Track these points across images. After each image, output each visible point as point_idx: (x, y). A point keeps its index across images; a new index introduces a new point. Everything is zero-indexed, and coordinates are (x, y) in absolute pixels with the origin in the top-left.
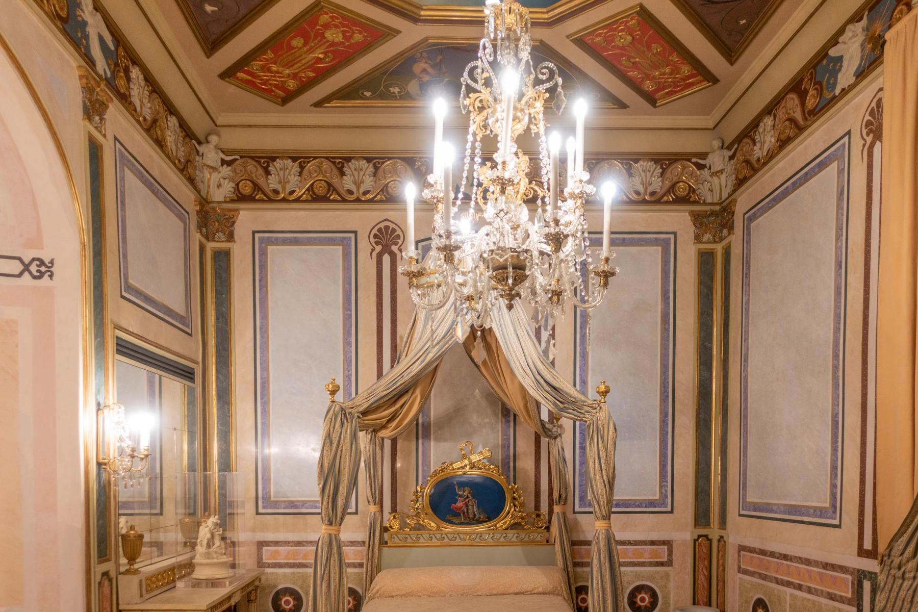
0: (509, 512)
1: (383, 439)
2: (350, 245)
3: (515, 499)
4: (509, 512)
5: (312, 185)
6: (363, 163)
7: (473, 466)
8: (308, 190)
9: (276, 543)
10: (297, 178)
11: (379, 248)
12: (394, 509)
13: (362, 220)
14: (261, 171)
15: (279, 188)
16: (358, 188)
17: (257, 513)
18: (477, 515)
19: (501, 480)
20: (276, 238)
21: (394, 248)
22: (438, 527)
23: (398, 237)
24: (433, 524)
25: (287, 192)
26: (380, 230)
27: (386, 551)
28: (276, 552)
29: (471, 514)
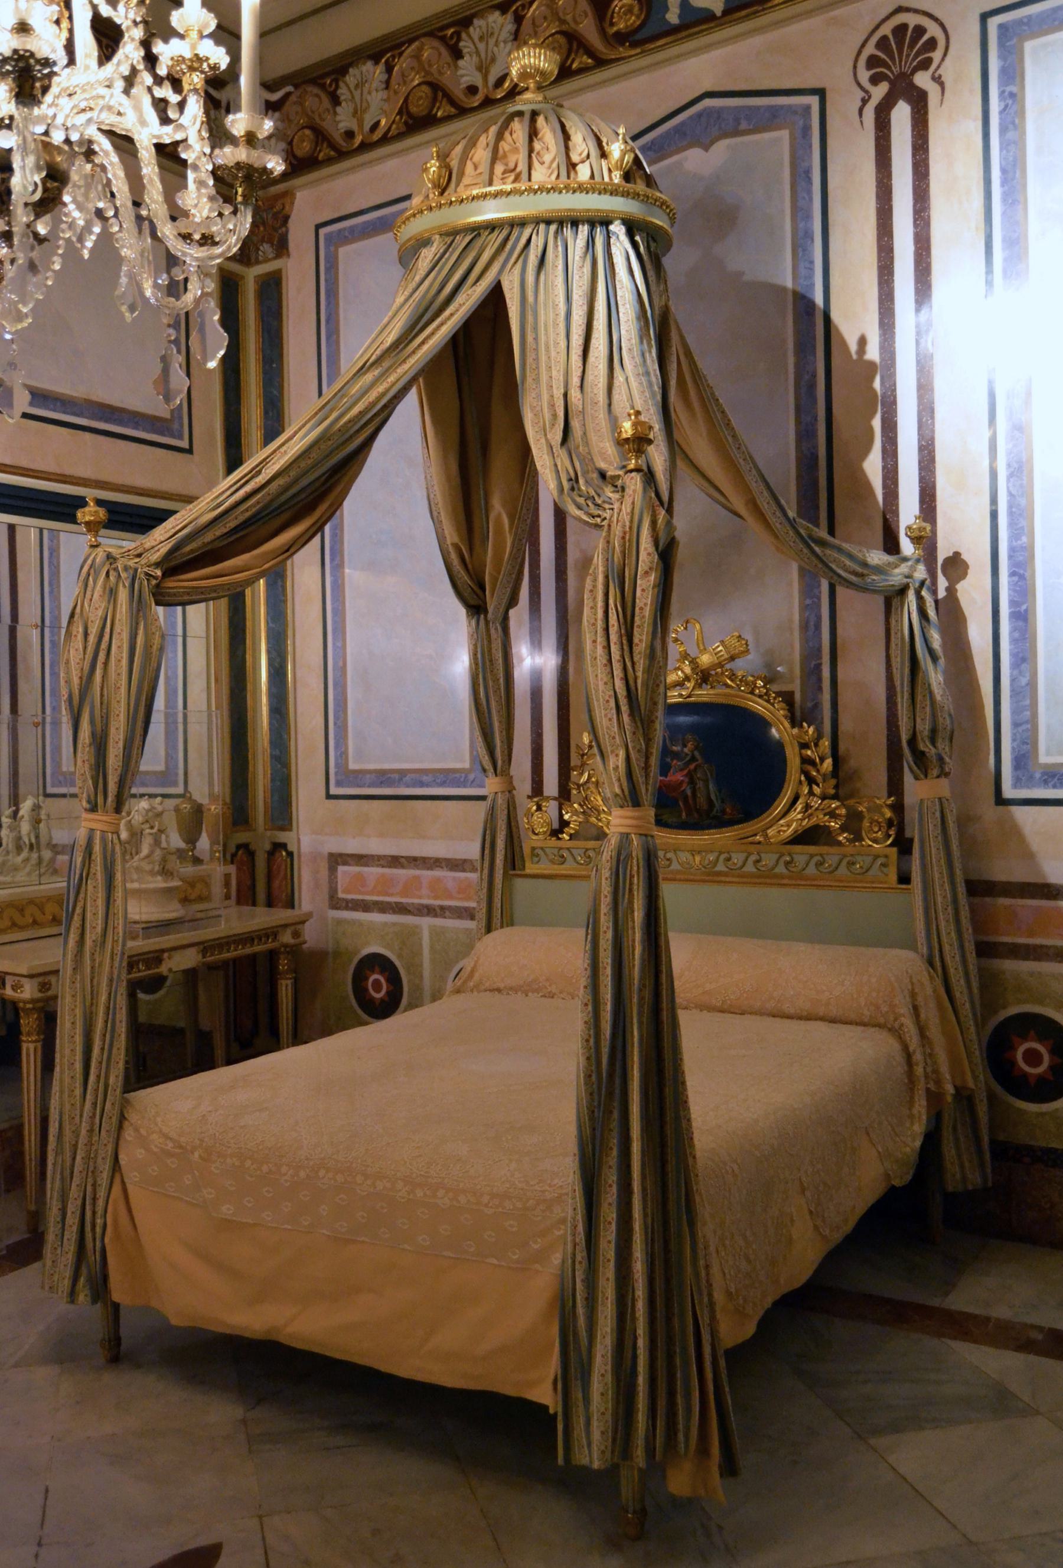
3: (806, 761)
9: (361, 859)
14: (326, 103)
15: (355, 127)
17: (329, 796)
18: (717, 804)
20: (352, 229)
27: (519, 884)
28: (360, 878)
29: (702, 800)
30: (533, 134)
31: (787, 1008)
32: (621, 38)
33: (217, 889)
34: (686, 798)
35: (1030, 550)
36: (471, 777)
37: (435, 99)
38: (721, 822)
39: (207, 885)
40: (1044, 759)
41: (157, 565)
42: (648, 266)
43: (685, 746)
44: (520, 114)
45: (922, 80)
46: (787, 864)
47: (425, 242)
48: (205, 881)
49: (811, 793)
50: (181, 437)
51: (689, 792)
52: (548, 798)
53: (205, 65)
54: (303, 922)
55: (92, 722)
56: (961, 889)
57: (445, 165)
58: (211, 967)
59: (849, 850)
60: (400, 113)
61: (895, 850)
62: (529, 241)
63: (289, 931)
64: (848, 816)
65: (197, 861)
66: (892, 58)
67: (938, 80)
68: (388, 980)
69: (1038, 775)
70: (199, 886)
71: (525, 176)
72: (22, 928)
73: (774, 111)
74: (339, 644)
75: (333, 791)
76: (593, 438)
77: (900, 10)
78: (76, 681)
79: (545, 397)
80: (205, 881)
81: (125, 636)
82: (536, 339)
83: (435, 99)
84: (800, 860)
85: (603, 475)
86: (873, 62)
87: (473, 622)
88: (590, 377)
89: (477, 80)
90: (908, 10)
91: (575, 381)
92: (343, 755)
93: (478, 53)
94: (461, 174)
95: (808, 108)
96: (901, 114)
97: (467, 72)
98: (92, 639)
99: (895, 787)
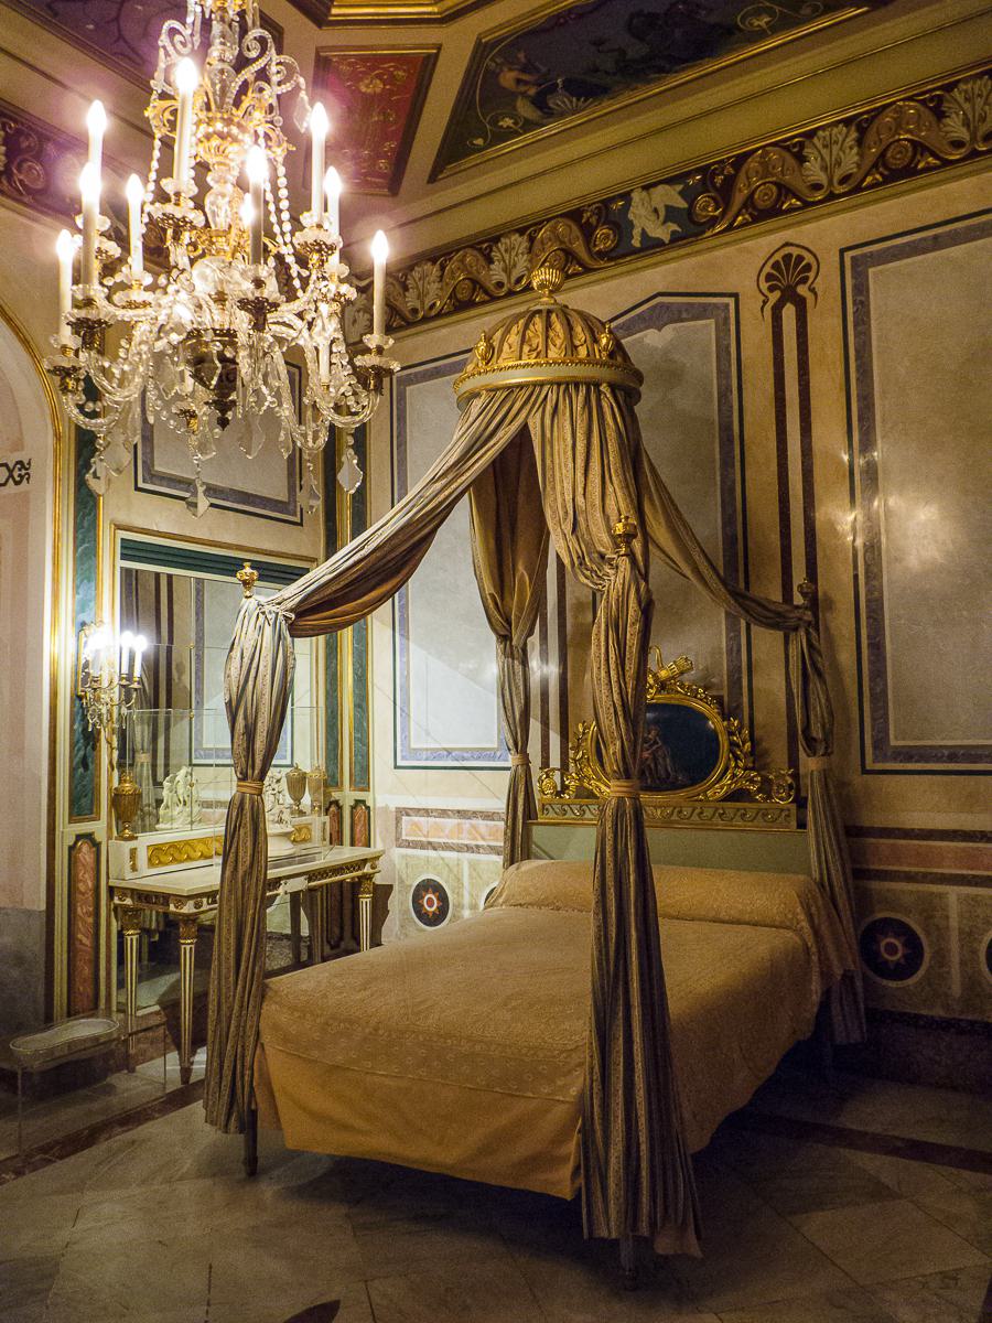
3: (732, 744)
6: (515, 238)
10: (437, 285)
17: (396, 767)
20: (416, 374)
25: (427, 307)
27: (534, 828)
30: (548, 326)
31: (723, 915)
32: (601, 255)
33: (316, 834)
34: (651, 769)
35: (880, 600)
36: (498, 754)
37: (474, 290)
38: (675, 786)
39: (309, 830)
40: (893, 742)
41: (291, 610)
42: (626, 413)
43: (649, 733)
44: (539, 312)
45: (802, 290)
46: (721, 815)
47: (477, 395)
48: (307, 827)
49: (737, 766)
50: (295, 514)
51: (652, 766)
52: (553, 770)
53: (342, 299)
54: (378, 858)
55: (245, 718)
56: (841, 832)
57: (490, 347)
58: (311, 890)
59: (764, 806)
60: (450, 298)
61: (795, 805)
62: (546, 396)
63: (368, 865)
64: (763, 782)
65: (302, 813)
66: (783, 276)
67: (812, 290)
68: (438, 899)
69: (889, 754)
70: (304, 831)
71: (543, 353)
72: (181, 862)
73: (705, 307)
74: (405, 660)
75: (399, 763)
76: (594, 529)
77: (787, 244)
78: (235, 689)
79: (559, 500)
80: (307, 827)
81: (270, 659)
82: (552, 461)
83: (474, 290)
84: (730, 813)
85: (602, 556)
86: (769, 277)
87: (502, 646)
88: (589, 488)
89: (504, 278)
90: (792, 245)
91: (580, 490)
92: (407, 738)
93: (504, 261)
94: (500, 350)
95: (727, 305)
96: (789, 312)
97: (496, 273)
98: (246, 660)
99: (793, 762)
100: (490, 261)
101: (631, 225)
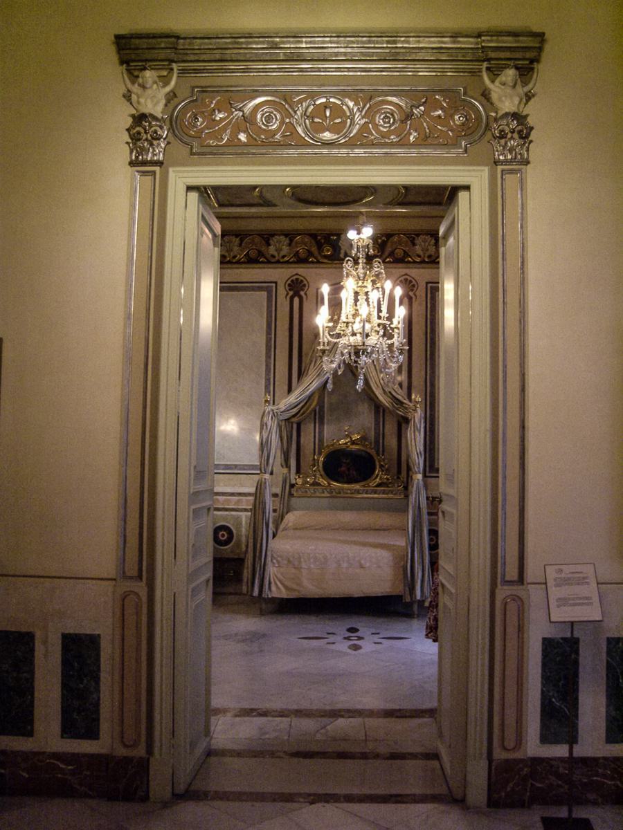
0: (378, 475)
1: (292, 423)
2: (272, 291)
4: (378, 475)
5: (248, 252)
6: (282, 238)
7: (353, 443)
8: (245, 255)
11: (291, 293)
12: (298, 471)
13: (281, 275)
16: (279, 254)
19: (373, 452)
21: (302, 293)
22: (329, 484)
23: (305, 285)
24: (325, 482)
26: (292, 281)
27: (293, 500)
32: (326, 257)
100: (269, 245)
101: (340, 249)
